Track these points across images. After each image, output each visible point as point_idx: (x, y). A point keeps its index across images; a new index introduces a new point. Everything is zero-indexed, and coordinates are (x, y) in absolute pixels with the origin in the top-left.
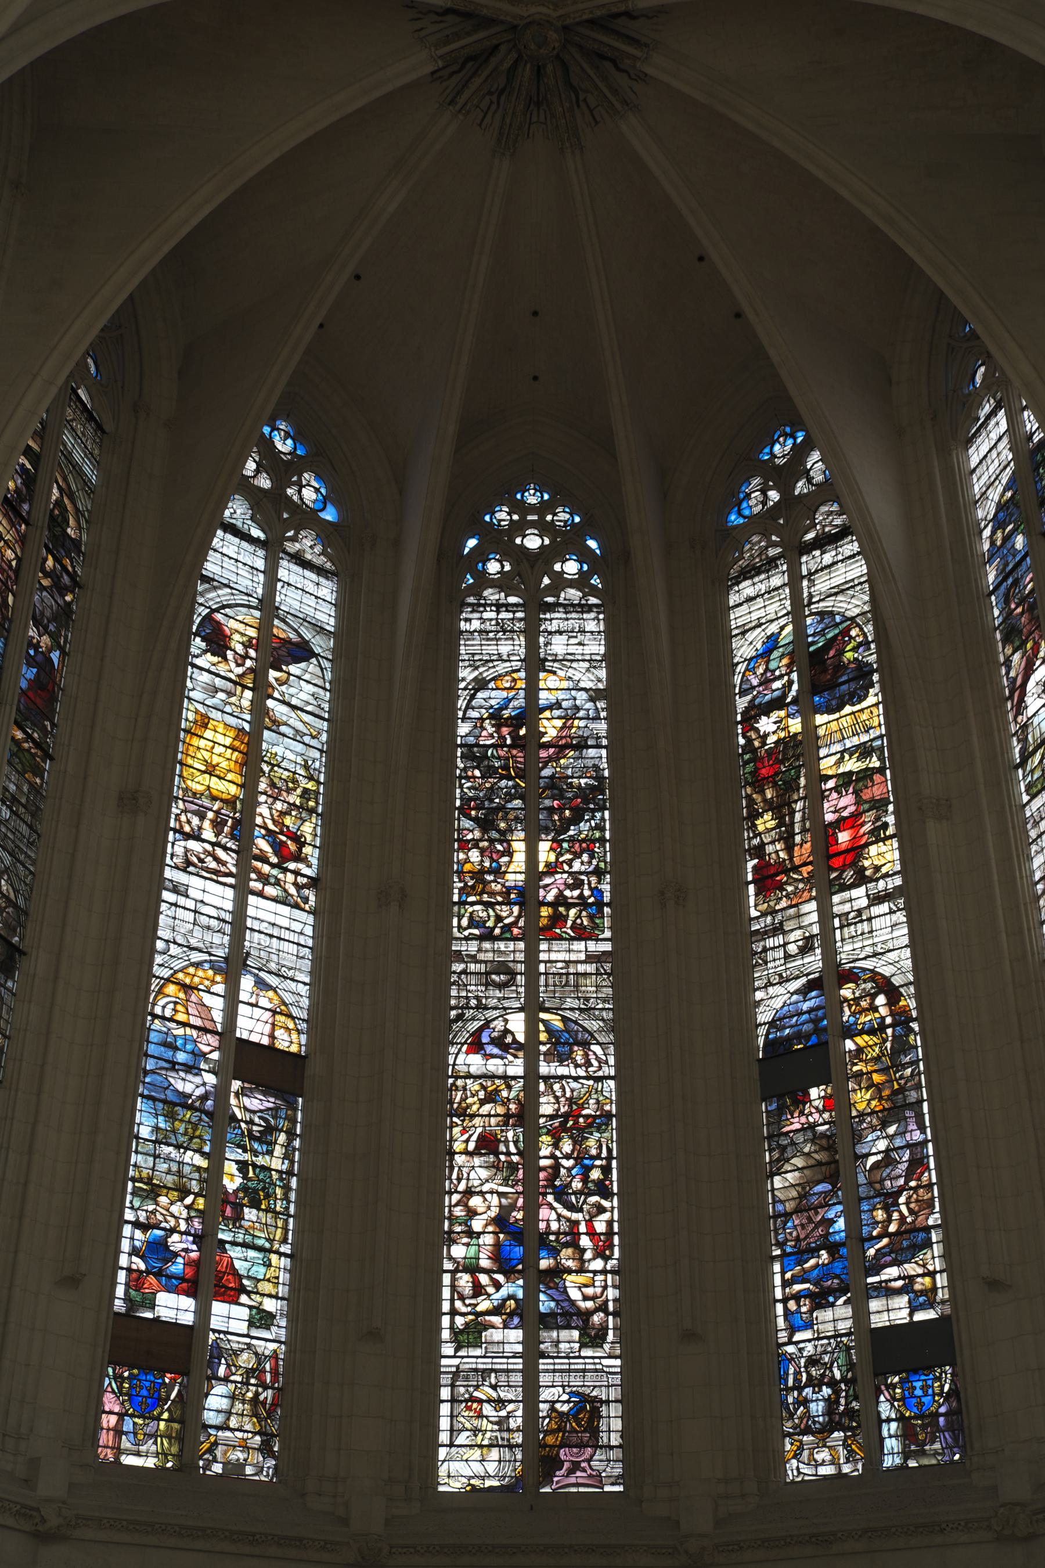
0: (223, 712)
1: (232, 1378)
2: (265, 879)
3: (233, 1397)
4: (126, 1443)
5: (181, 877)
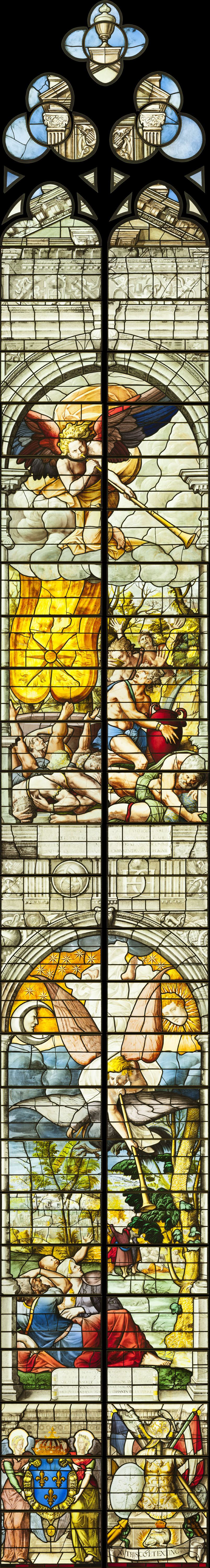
0: (58, 563)
1: (142, 1453)
2: (130, 797)
5: (26, 833)
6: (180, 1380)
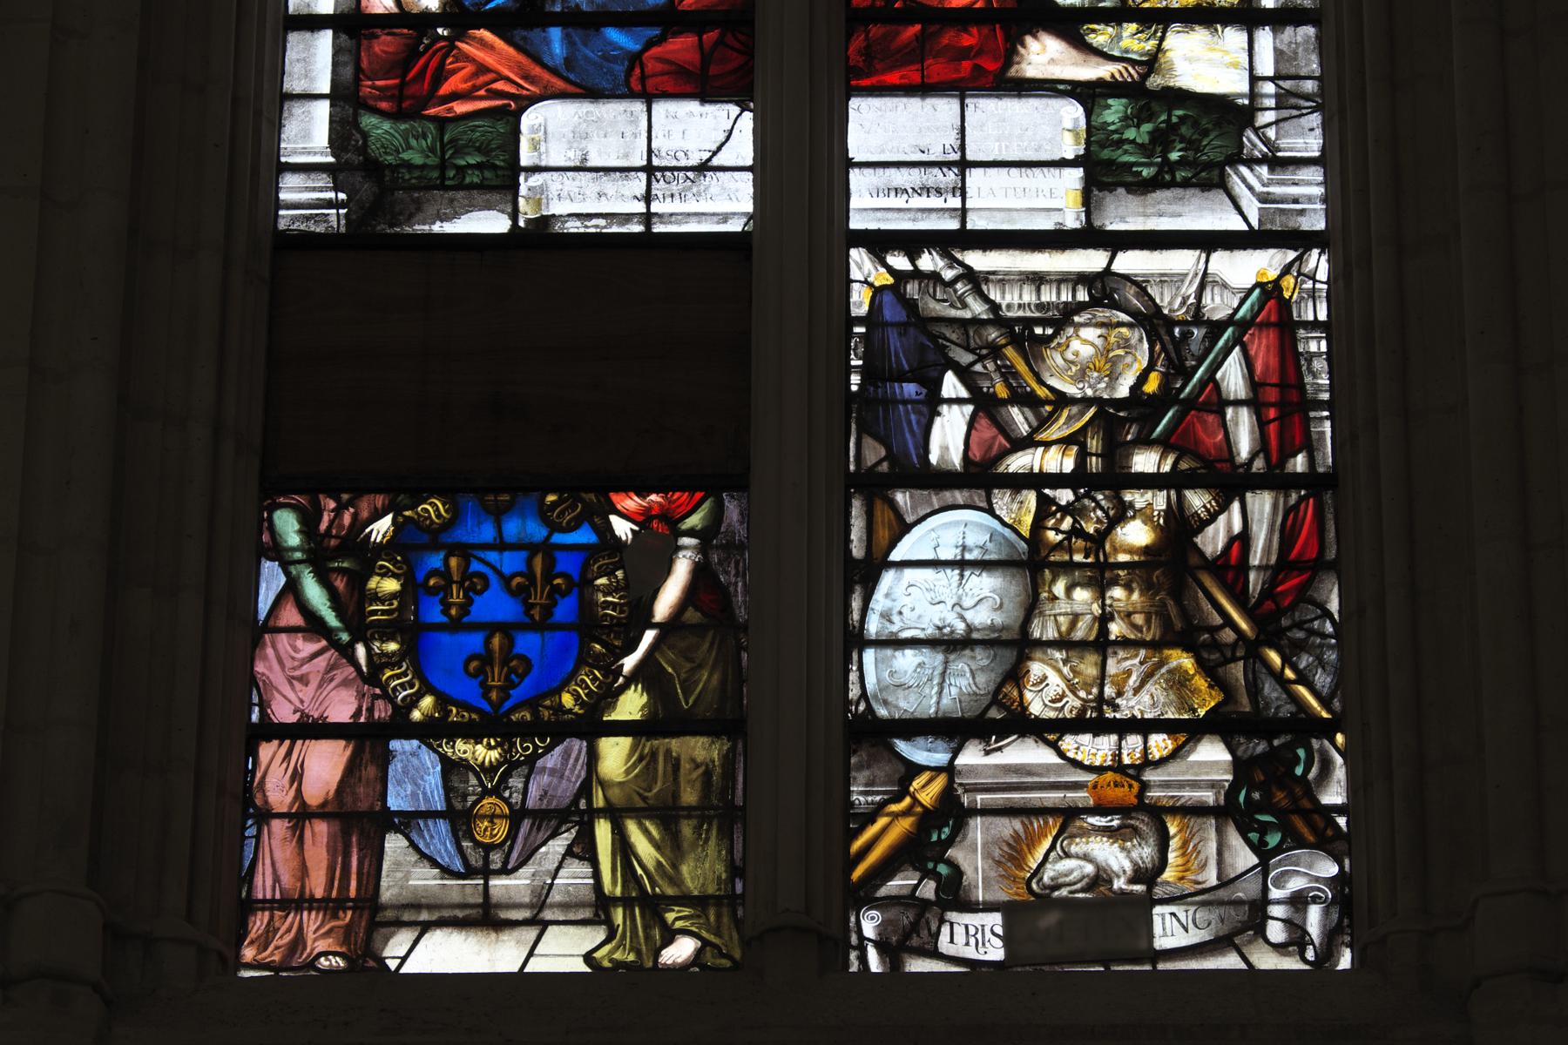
3: (1030, 563)
4: (404, 871)
6: (1191, 145)
